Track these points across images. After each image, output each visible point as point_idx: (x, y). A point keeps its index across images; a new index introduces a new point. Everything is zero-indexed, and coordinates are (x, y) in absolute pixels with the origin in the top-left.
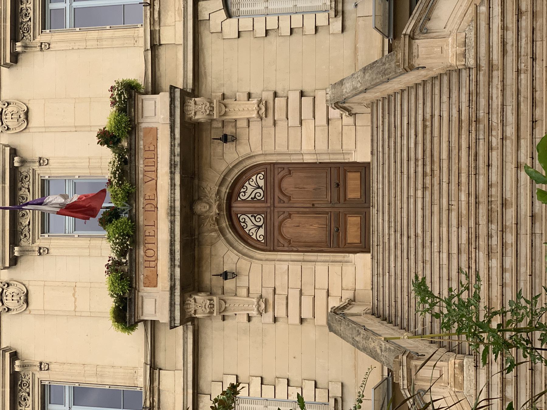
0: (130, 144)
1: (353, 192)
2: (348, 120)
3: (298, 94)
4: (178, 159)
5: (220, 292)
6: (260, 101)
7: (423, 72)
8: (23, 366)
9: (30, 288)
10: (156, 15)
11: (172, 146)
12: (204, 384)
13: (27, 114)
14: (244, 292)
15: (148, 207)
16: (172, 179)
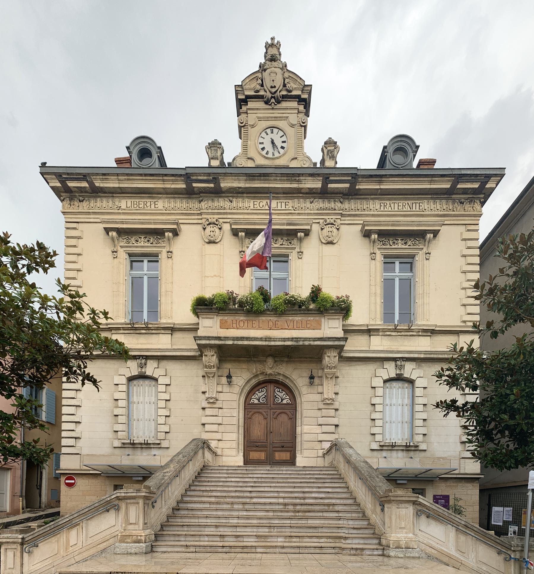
1: (278, 456)
2: (321, 453)
3: (336, 423)
5: (219, 374)
12: (164, 363)
14: (220, 389)
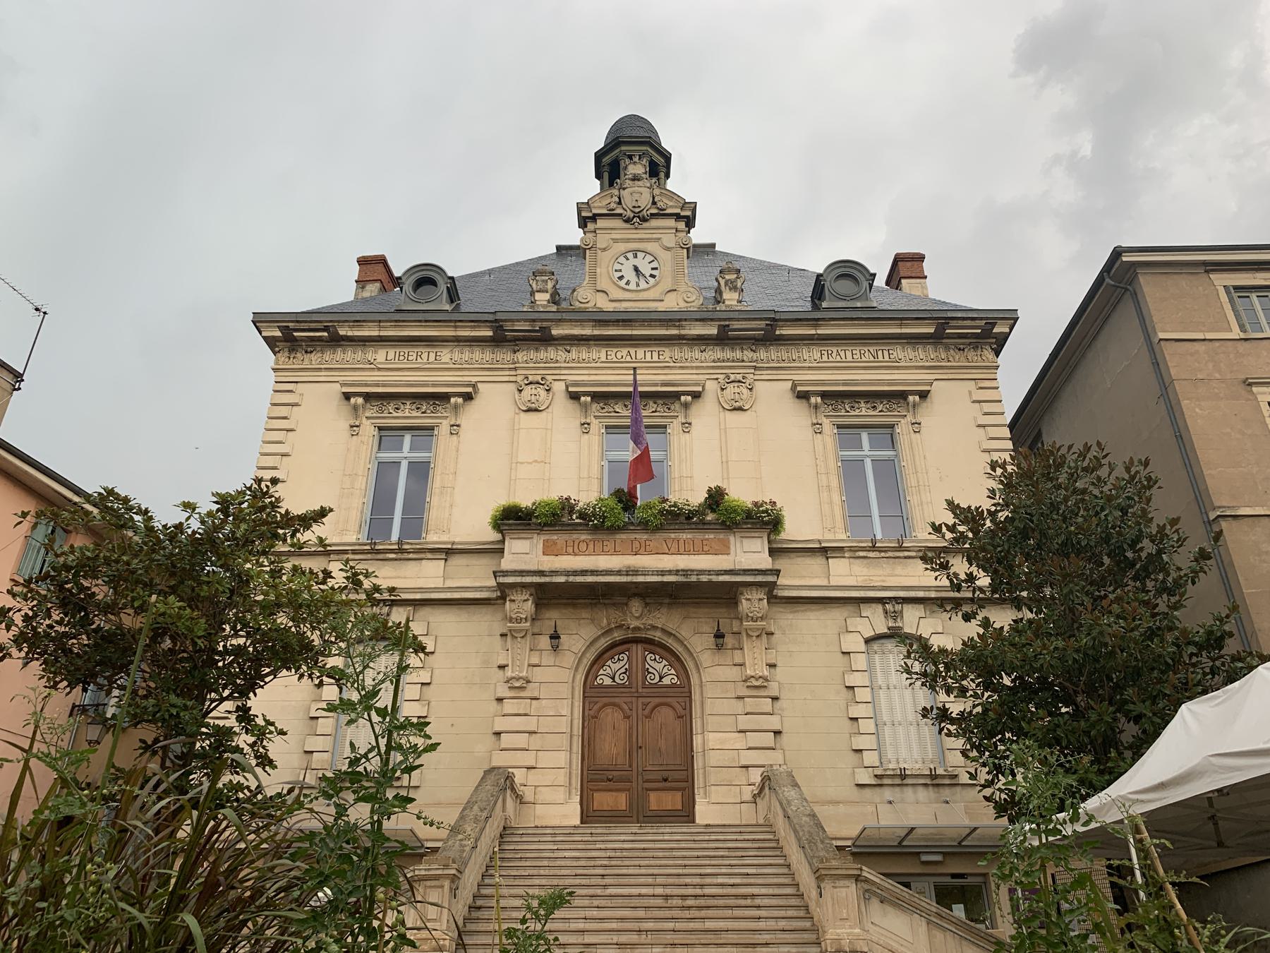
0: (709, 523)
2: (747, 793)
3: (777, 727)
4: (694, 578)
5: (536, 631)
6: (767, 680)
7: (814, 893)
8: (456, 407)
9: (544, 413)
10: (861, 554)
11: (709, 572)
12: (425, 612)
13: (740, 409)
14: (535, 660)
15: (636, 544)
16: (670, 572)
